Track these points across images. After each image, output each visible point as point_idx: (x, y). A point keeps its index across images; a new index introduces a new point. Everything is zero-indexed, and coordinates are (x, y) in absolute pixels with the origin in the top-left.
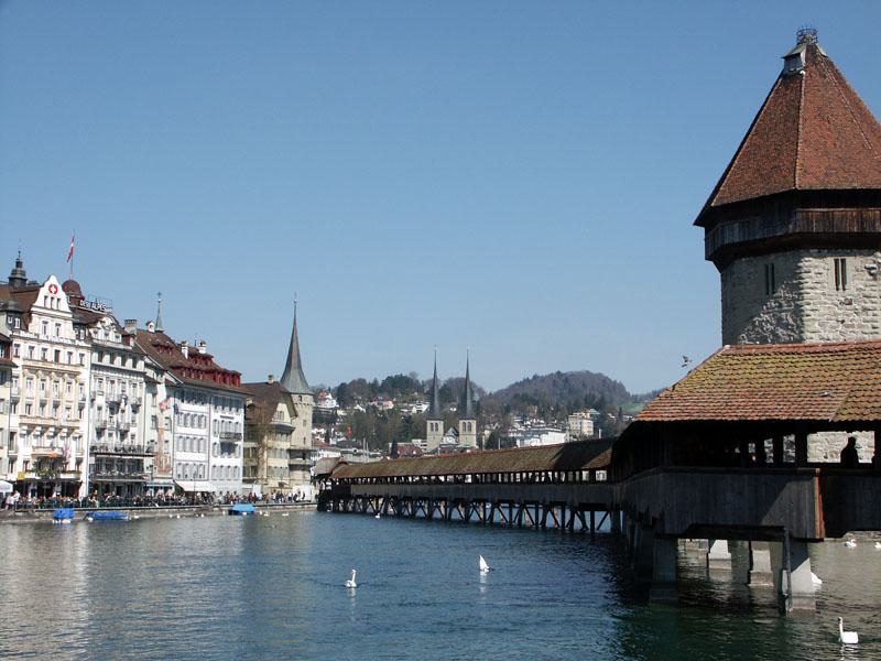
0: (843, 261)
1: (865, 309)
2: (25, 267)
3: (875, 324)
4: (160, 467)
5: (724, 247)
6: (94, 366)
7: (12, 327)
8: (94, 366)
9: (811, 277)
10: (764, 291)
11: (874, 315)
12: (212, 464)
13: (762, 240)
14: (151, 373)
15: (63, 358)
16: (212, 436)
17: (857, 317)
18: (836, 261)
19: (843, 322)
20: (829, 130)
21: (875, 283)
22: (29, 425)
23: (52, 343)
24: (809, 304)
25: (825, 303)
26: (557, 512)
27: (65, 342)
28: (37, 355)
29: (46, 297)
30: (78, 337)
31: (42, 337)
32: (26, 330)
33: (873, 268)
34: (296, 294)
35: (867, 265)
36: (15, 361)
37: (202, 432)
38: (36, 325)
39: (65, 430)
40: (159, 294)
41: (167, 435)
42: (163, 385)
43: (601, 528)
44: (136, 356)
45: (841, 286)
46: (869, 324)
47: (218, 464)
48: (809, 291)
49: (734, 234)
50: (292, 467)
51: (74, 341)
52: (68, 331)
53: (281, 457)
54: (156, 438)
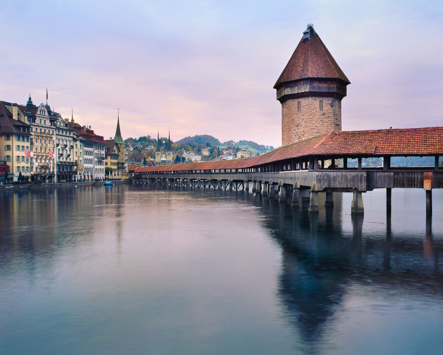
0: (322, 101)
1: (329, 117)
2: (32, 100)
3: (332, 122)
4: (79, 169)
5: (285, 96)
6: (57, 134)
7: (29, 121)
8: (57, 134)
9: (312, 106)
10: (297, 110)
11: (331, 119)
12: (95, 168)
14: (75, 137)
15: (47, 131)
16: (95, 158)
18: (320, 101)
19: (322, 120)
20: (318, 58)
21: (332, 108)
22: (37, 155)
23: (43, 127)
24: (312, 115)
25: (317, 115)
27: (47, 126)
28: (39, 131)
29: (40, 111)
31: (40, 125)
32: (35, 122)
33: (331, 103)
35: (329, 103)
36: (31, 133)
38: (37, 121)
39: (44, 157)
40: (72, 109)
42: (79, 141)
44: (70, 131)
45: (321, 109)
46: (329, 122)
47: (97, 168)
49: (288, 91)
50: (118, 168)
51: (50, 126)
52: (48, 123)
53: (115, 165)
54: (77, 159)
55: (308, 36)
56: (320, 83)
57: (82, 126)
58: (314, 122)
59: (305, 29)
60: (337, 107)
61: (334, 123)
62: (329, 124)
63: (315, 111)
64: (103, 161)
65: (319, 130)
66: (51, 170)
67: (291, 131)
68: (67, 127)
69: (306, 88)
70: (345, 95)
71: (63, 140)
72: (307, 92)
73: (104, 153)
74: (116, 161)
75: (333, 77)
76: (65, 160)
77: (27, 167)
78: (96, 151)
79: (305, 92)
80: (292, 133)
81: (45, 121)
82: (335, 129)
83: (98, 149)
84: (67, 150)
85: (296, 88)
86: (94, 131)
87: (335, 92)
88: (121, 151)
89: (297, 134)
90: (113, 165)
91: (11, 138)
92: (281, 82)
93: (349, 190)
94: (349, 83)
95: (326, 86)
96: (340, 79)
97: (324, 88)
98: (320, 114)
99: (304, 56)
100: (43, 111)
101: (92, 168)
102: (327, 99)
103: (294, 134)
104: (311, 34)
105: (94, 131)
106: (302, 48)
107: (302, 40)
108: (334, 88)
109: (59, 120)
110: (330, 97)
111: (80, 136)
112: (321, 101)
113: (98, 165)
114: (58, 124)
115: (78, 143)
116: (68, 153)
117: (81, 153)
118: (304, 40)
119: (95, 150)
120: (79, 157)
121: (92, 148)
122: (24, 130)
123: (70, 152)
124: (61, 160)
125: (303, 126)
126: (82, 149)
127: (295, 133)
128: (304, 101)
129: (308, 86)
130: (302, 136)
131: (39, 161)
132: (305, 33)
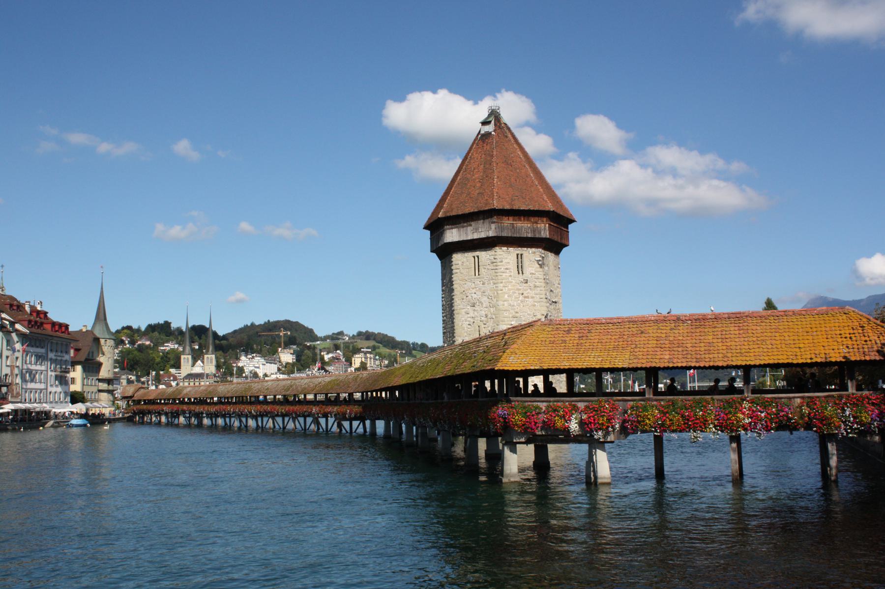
0: (521, 255)
3: (541, 296)
4: (12, 394)
9: (503, 265)
13: (472, 241)
16: (49, 371)
17: (530, 292)
18: (517, 255)
19: (523, 294)
21: (541, 270)
25: (512, 282)
26: (301, 420)
33: (540, 260)
34: (102, 267)
35: (536, 259)
40: (2, 266)
43: (358, 431)
45: (521, 272)
46: (538, 296)
48: (501, 274)
49: (452, 235)
56: (516, 221)
57: (22, 301)
58: (506, 296)
59: (484, 115)
60: (552, 268)
61: (546, 298)
62: (536, 301)
63: (507, 275)
65: (517, 313)
67: (461, 316)
72: (492, 237)
73: (68, 359)
75: (541, 209)
79: (488, 238)
80: (463, 319)
82: (549, 311)
85: (469, 228)
86: (47, 313)
87: (545, 239)
88: (106, 353)
89: (472, 321)
92: (439, 216)
93: (580, 438)
94: (572, 221)
95: (529, 225)
96: (556, 213)
97: (524, 228)
98: (518, 282)
99: (484, 167)
102: (531, 252)
103: (466, 320)
104: (495, 125)
105: (47, 313)
106: (480, 150)
107: (480, 136)
108: (545, 229)
110: (537, 247)
111: (17, 323)
112: (520, 256)
118: (483, 135)
119: (49, 352)
121: (42, 348)
125: (484, 306)
127: (469, 319)
128: (484, 256)
130: (483, 326)
132: (485, 123)
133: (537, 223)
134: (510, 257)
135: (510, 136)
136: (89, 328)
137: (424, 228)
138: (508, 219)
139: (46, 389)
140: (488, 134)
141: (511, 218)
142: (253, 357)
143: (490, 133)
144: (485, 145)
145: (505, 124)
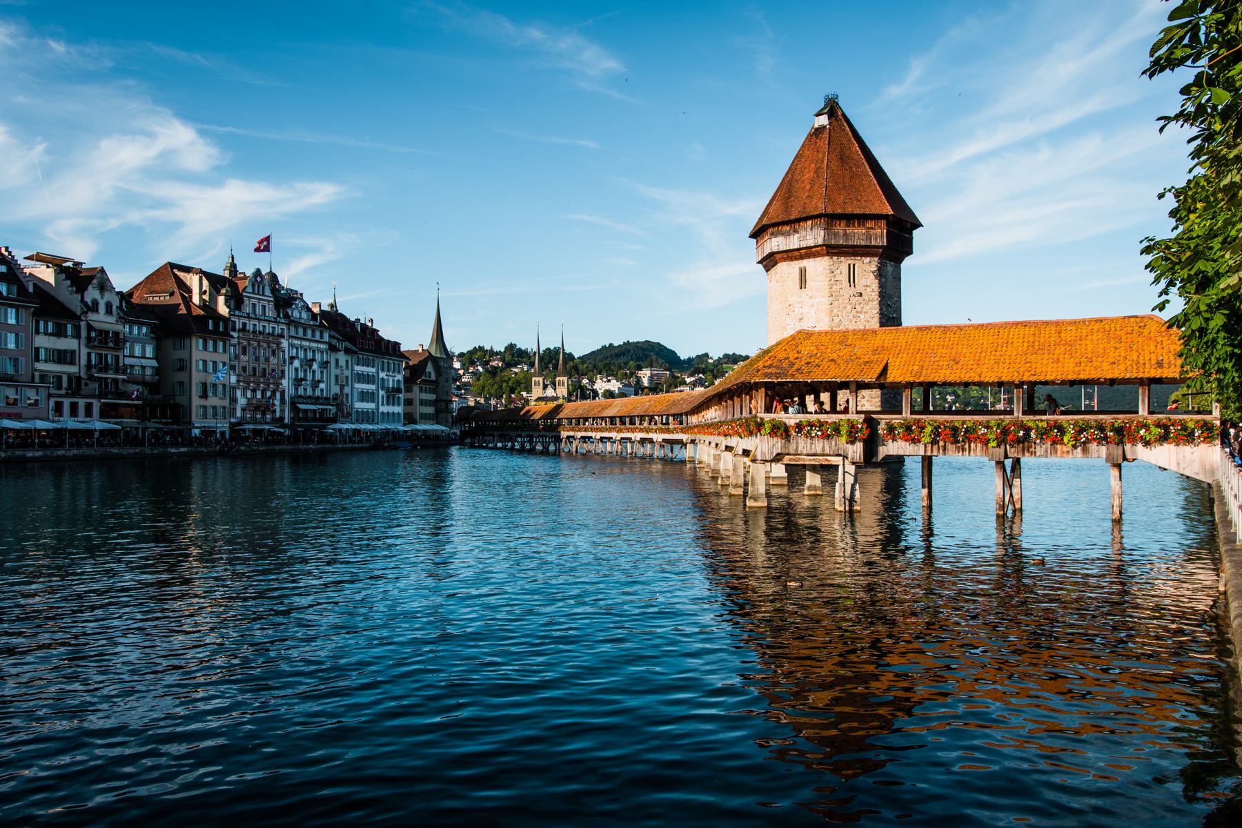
0: (854, 265)
4: (343, 414)
5: (771, 255)
10: (798, 286)
12: (380, 411)
14: (334, 342)
18: (849, 265)
23: (259, 319)
27: (269, 319)
30: (279, 316)
36: (232, 333)
37: (372, 387)
41: (347, 390)
47: (385, 411)
49: (776, 243)
50: (436, 411)
52: (270, 313)
53: (430, 406)
55: (823, 120)
57: (353, 319)
64: (399, 397)
66: (278, 414)
68: (317, 321)
69: (812, 236)
70: (909, 252)
71: (305, 350)
72: (820, 246)
74: (432, 397)
76: (309, 392)
77: (224, 408)
78: (382, 375)
81: (264, 307)
83: (388, 371)
84: (314, 372)
85: (796, 236)
90: (426, 405)
91: (187, 341)
94: (918, 225)
97: (858, 235)
100: (258, 286)
101: (373, 412)
108: (882, 236)
109: (296, 304)
112: (852, 266)
113: (388, 404)
114: (296, 314)
115: (342, 357)
116: (318, 377)
117: (347, 377)
118: (817, 129)
120: (342, 387)
121: (373, 367)
122: (216, 326)
123: (322, 377)
124: (301, 391)
126: (350, 370)
128: (812, 265)
129: (822, 233)
131: (249, 395)
133: (872, 228)
134: (841, 267)
135: (848, 129)
136: (425, 348)
137: (751, 237)
138: (840, 225)
139: (378, 409)
140: (821, 129)
141: (843, 224)
142: (609, 381)
143: (825, 127)
144: (818, 141)
145: (844, 115)
